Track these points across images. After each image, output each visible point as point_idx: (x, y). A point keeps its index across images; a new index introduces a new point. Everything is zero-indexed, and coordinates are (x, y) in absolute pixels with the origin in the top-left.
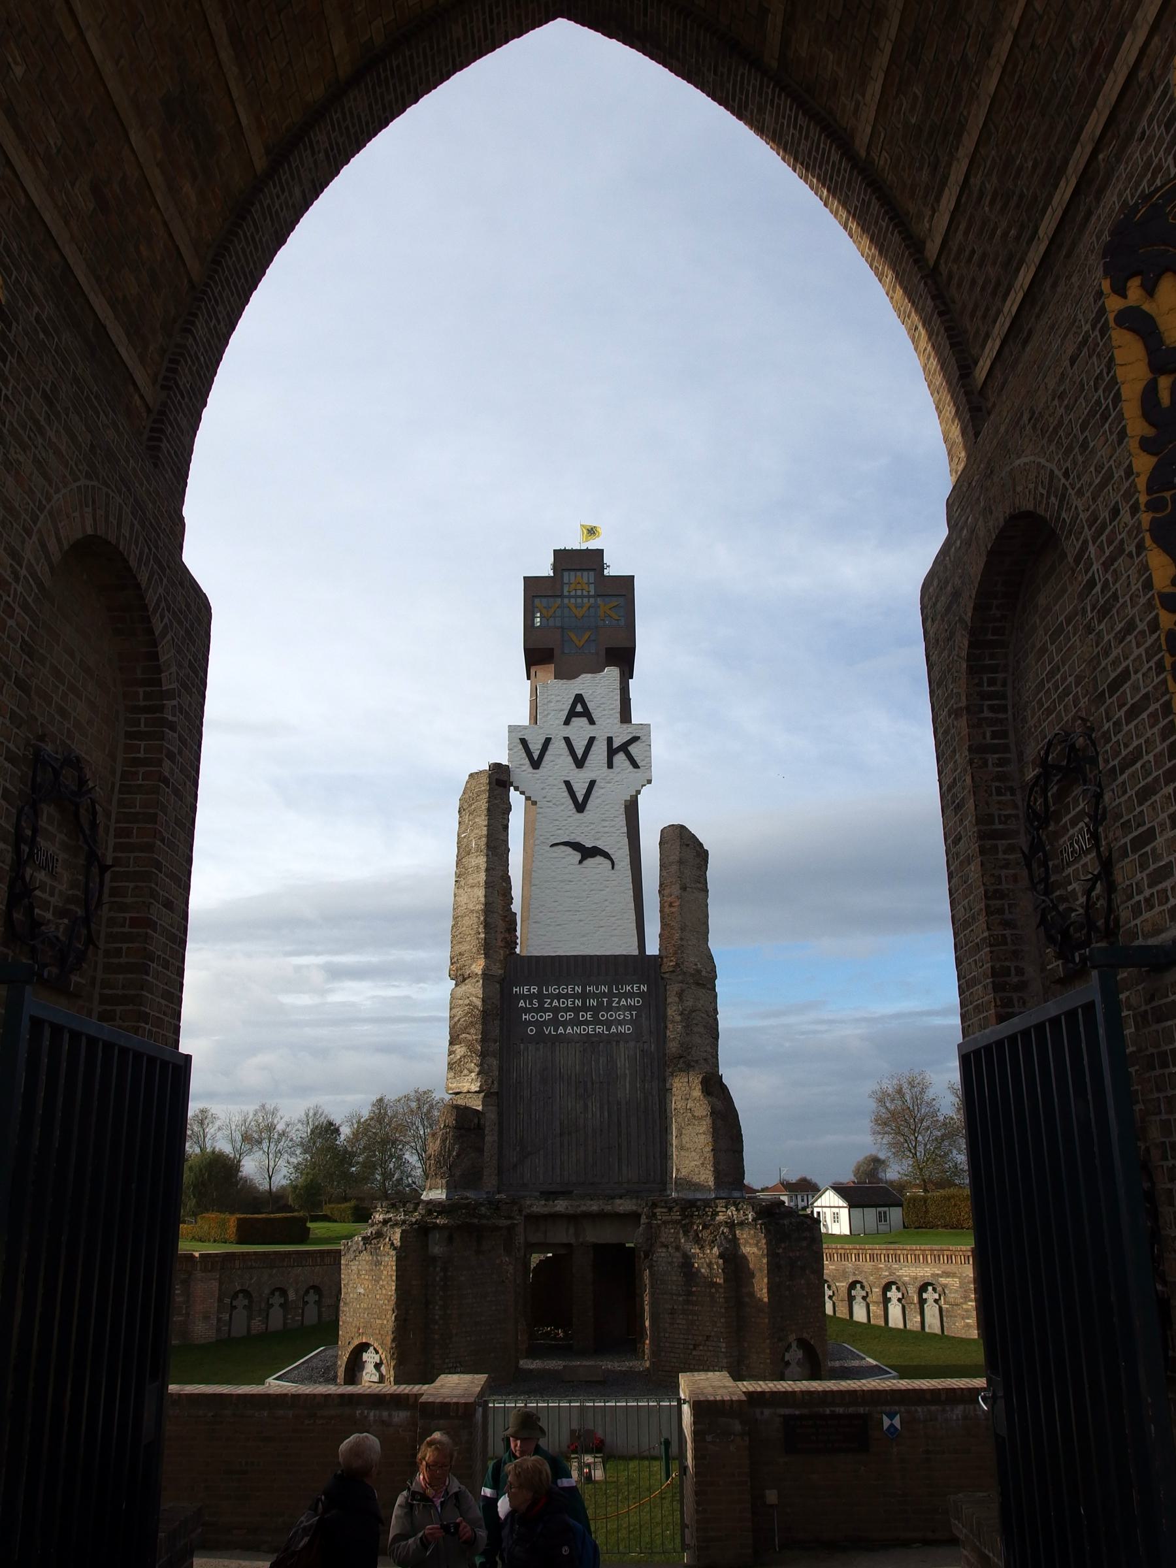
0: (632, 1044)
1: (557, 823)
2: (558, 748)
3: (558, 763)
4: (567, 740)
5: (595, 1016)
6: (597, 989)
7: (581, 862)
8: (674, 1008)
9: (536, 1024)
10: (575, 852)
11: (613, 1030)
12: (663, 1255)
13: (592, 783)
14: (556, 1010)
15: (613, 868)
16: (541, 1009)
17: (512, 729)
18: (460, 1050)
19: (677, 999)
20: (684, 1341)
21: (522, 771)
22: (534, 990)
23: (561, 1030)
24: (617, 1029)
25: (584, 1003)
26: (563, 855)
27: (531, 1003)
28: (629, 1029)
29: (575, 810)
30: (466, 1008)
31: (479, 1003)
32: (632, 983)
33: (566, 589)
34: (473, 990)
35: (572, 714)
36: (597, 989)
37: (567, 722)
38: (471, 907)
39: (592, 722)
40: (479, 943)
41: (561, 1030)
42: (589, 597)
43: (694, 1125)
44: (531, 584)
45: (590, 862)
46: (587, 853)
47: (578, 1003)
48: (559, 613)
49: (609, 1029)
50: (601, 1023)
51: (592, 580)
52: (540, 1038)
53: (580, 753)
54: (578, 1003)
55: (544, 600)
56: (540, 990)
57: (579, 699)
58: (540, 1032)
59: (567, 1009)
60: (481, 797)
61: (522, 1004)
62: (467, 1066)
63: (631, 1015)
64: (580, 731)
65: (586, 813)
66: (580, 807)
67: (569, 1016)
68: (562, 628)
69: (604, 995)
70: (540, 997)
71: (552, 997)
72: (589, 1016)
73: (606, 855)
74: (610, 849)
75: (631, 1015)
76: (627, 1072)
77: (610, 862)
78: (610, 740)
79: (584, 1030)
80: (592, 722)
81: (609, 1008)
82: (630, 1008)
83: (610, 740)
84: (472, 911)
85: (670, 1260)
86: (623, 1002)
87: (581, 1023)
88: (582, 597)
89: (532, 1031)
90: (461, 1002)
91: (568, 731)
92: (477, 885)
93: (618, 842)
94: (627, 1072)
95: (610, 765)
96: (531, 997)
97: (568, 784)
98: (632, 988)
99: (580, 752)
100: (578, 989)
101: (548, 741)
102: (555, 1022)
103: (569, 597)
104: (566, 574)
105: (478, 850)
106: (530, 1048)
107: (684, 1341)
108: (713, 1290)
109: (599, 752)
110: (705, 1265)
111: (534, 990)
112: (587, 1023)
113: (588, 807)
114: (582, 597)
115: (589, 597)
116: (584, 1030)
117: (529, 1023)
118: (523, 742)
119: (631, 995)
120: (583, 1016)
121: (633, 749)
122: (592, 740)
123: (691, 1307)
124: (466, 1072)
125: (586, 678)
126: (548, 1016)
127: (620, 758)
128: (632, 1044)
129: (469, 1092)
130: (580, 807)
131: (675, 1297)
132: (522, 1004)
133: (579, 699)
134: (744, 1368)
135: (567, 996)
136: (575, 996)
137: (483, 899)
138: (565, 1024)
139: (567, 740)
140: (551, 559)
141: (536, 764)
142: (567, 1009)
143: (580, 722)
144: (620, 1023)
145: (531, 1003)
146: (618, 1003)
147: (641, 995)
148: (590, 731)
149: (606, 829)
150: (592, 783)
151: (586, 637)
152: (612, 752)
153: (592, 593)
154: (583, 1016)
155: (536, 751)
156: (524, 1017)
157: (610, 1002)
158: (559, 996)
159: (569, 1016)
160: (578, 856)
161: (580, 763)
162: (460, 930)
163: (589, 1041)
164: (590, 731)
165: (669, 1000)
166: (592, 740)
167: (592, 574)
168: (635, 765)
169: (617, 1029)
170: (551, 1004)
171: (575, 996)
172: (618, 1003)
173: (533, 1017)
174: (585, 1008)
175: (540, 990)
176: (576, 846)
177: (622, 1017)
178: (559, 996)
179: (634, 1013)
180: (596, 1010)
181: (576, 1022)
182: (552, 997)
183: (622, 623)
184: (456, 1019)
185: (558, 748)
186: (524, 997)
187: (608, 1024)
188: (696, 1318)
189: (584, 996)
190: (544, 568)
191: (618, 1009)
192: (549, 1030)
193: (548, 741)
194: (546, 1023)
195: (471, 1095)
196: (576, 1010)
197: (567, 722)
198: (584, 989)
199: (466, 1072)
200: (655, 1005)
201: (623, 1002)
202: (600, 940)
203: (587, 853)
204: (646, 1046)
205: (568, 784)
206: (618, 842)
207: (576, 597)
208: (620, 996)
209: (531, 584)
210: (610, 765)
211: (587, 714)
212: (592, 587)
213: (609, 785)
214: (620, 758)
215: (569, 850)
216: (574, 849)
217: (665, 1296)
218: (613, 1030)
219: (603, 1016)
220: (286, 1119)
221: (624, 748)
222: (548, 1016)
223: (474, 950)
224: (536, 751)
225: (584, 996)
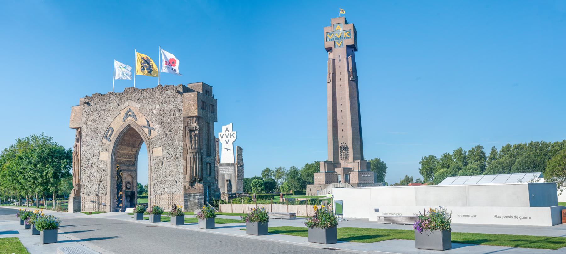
2: (225, 136)
4: (226, 134)
9: (222, 172)
13: (229, 140)
14: (224, 170)
35: (226, 131)
37: (226, 132)
39: (229, 131)
45: (228, 151)
46: (228, 149)
52: (222, 174)
53: (227, 136)
57: (227, 128)
66: (227, 143)
70: (222, 169)
73: (230, 150)
78: (231, 134)
80: (229, 131)
83: (231, 134)
87: (226, 172)
89: (221, 173)
91: (226, 133)
95: (231, 137)
97: (226, 140)
99: (227, 136)
100: (226, 168)
101: (223, 135)
102: (224, 172)
109: (230, 135)
115: (341, 31)
119: (232, 168)
122: (229, 134)
125: (228, 125)
127: (232, 136)
130: (227, 143)
133: (227, 128)
139: (226, 134)
141: (222, 138)
143: (227, 132)
148: (228, 133)
150: (229, 140)
152: (231, 136)
153: (342, 30)
155: (222, 136)
159: (225, 171)
160: (227, 150)
163: (228, 174)
164: (228, 133)
166: (229, 134)
168: (234, 137)
176: (227, 149)
180: (228, 170)
185: (225, 136)
189: (227, 168)
192: (223, 173)
193: (223, 135)
197: (226, 132)
203: (228, 149)
205: (226, 140)
210: (231, 137)
211: (228, 130)
214: (232, 136)
219: (229, 171)
220: (287, 170)
221: (233, 135)
224: (222, 136)
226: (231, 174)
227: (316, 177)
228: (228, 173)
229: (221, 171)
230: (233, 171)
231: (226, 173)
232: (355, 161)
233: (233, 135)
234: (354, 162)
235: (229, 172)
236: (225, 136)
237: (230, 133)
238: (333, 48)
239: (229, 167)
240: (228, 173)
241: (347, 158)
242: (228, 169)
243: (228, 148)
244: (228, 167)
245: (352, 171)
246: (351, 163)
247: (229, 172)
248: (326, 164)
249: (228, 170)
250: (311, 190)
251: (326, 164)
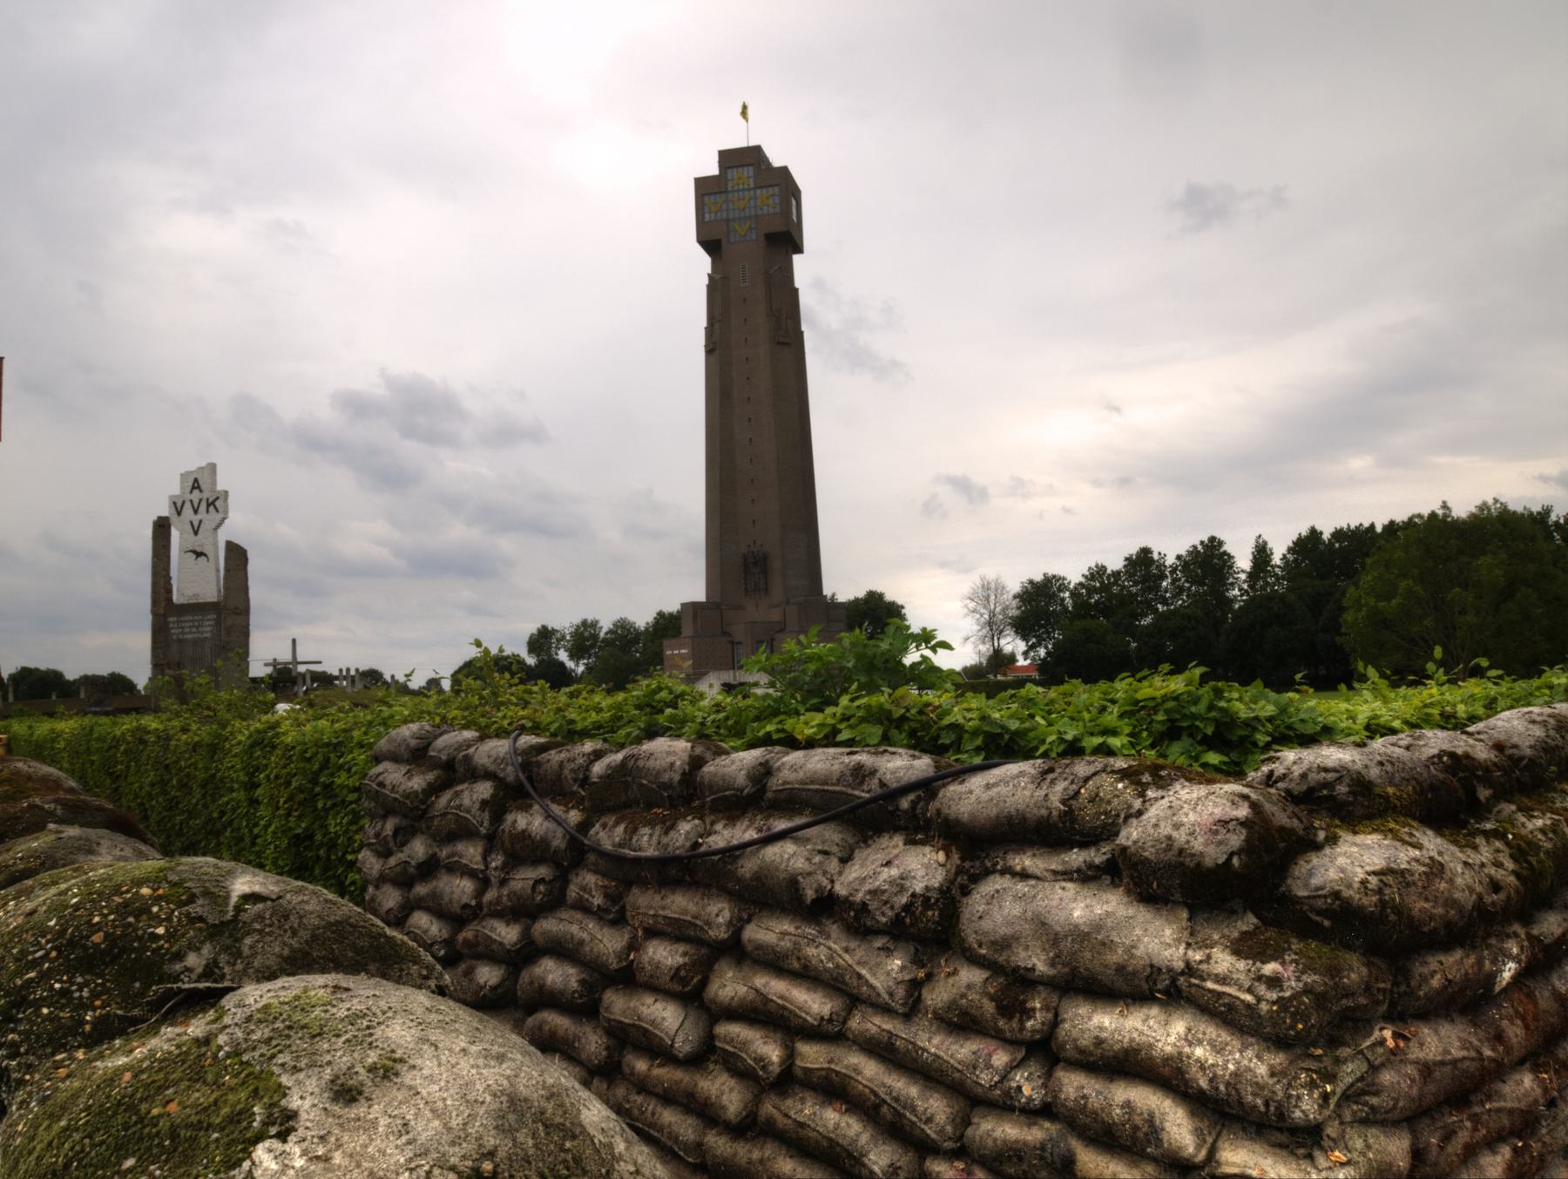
2: (188, 505)
3: (188, 510)
13: (201, 521)
17: (171, 497)
21: (174, 519)
33: (730, 185)
35: (193, 488)
42: (749, 189)
44: (700, 182)
46: (199, 554)
48: (724, 207)
51: (751, 173)
52: (180, 641)
55: (712, 197)
57: (196, 480)
64: (196, 495)
66: (196, 533)
68: (728, 220)
73: (205, 555)
88: (743, 190)
101: (184, 502)
102: (183, 633)
103: (733, 191)
104: (729, 171)
109: (204, 505)
114: (743, 190)
115: (749, 189)
118: (175, 503)
121: (217, 503)
122: (201, 500)
127: (212, 508)
130: (196, 533)
133: (196, 480)
140: (716, 158)
141: (179, 513)
143: (196, 492)
150: (201, 521)
151: (747, 226)
152: (208, 505)
161: (196, 511)
163: (196, 642)
167: (751, 168)
168: (217, 511)
176: (194, 552)
180: (197, 627)
181: (190, 633)
183: (778, 210)
185: (188, 505)
187: (202, 633)
189: (193, 621)
190: (712, 169)
193: (184, 502)
203: (199, 554)
207: (739, 191)
209: (700, 182)
211: (199, 487)
212: (751, 182)
214: (212, 508)
221: (213, 503)
225: (193, 621)
227: (669, 652)
228: (195, 636)
231: (188, 636)
233: (213, 503)
236: (188, 510)
237: (206, 495)
238: (724, 242)
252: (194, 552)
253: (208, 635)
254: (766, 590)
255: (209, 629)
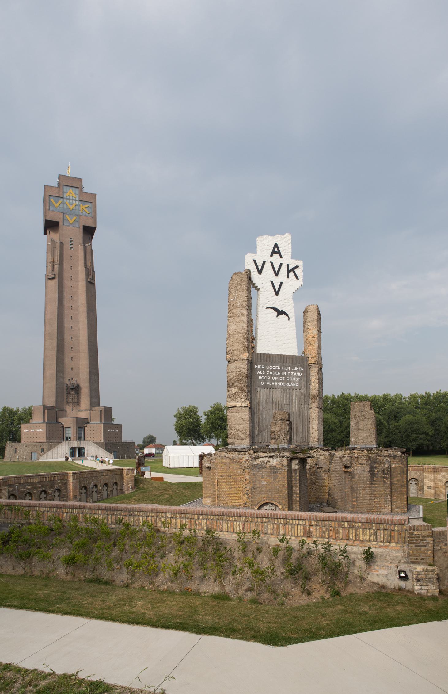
0: (298, 390)
1: (268, 299)
5: (285, 379)
6: (286, 368)
7: (277, 316)
8: (315, 377)
9: (264, 380)
10: (275, 312)
11: (292, 384)
12: (359, 467)
14: (271, 376)
15: (289, 320)
16: (265, 375)
18: (234, 390)
19: (317, 374)
20: (370, 497)
22: (263, 367)
23: (273, 384)
24: (293, 384)
25: (281, 373)
26: (270, 313)
27: (262, 372)
28: (297, 384)
29: (275, 294)
30: (237, 373)
31: (246, 372)
32: (298, 366)
34: (242, 366)
36: (286, 368)
38: (238, 330)
40: (244, 346)
41: (273, 384)
43: (365, 421)
45: (280, 316)
47: (279, 373)
49: (290, 384)
50: (288, 382)
52: (265, 387)
54: (279, 373)
56: (265, 368)
58: (266, 384)
59: (275, 376)
60: (242, 283)
61: (258, 372)
62: (239, 396)
63: (298, 379)
65: (279, 296)
66: (277, 293)
67: (276, 378)
69: (288, 371)
70: (265, 370)
71: (270, 370)
72: (283, 379)
73: (287, 315)
74: (288, 312)
75: (298, 379)
76: (296, 401)
77: (288, 317)
79: (281, 384)
81: (290, 376)
82: (298, 376)
84: (240, 333)
85: (363, 469)
86: (295, 374)
89: (262, 383)
90: (233, 370)
92: (243, 322)
93: (291, 310)
94: (296, 401)
96: (262, 370)
98: (298, 369)
100: (279, 368)
102: (272, 381)
105: (242, 307)
106: (262, 390)
107: (370, 497)
108: (385, 479)
110: (381, 471)
111: (263, 367)
112: (282, 381)
113: (280, 293)
116: (281, 384)
117: (261, 380)
119: (297, 371)
120: (281, 379)
123: (374, 485)
124: (238, 398)
126: (268, 378)
128: (298, 390)
129: (241, 406)
130: (277, 293)
131: (365, 482)
132: (258, 372)
134: (394, 505)
135: (275, 370)
136: (278, 370)
137: (246, 328)
138: (274, 381)
142: (275, 376)
144: (294, 382)
145: (262, 372)
146: (293, 374)
147: (301, 372)
149: (286, 304)
154: (281, 379)
156: (259, 378)
157: (291, 374)
158: (272, 370)
159: (276, 378)
160: (276, 314)
162: (232, 340)
163: (284, 389)
165: (312, 374)
169: (293, 384)
170: (269, 373)
171: (278, 370)
172: (293, 374)
173: (263, 378)
174: (281, 376)
175: (265, 368)
176: (276, 309)
177: (295, 380)
178: (272, 370)
179: (299, 378)
180: (286, 376)
181: (279, 381)
182: (270, 370)
184: (231, 377)
186: (260, 370)
187: (290, 382)
188: (376, 489)
189: (281, 371)
191: (294, 376)
192: (269, 383)
194: (267, 381)
195: (241, 408)
196: (278, 376)
198: (281, 368)
199: (238, 398)
200: (306, 375)
201: (295, 374)
202: (284, 349)
203: (280, 313)
204: (303, 391)
206: (291, 310)
208: (294, 371)
213: (287, 285)
215: (273, 311)
216: (275, 311)
217: (360, 482)
218: (292, 384)
219: (288, 379)
222: (268, 378)
223: (241, 349)
225: (281, 371)
226: (293, 388)
228: (283, 384)
229: (260, 378)
230: (299, 382)
232: (93, 408)
234: (91, 409)
235: (287, 384)
236: (268, 270)
239: (288, 368)
240: (283, 384)
241: (78, 403)
242: (284, 373)
243: (280, 309)
244: (284, 368)
245: (88, 423)
246: (86, 410)
247: (287, 384)
248: (46, 411)
249: (286, 376)
250: (18, 451)
251: (46, 411)
252: (276, 309)
253: (296, 384)
254: (78, 402)
255: (296, 379)
